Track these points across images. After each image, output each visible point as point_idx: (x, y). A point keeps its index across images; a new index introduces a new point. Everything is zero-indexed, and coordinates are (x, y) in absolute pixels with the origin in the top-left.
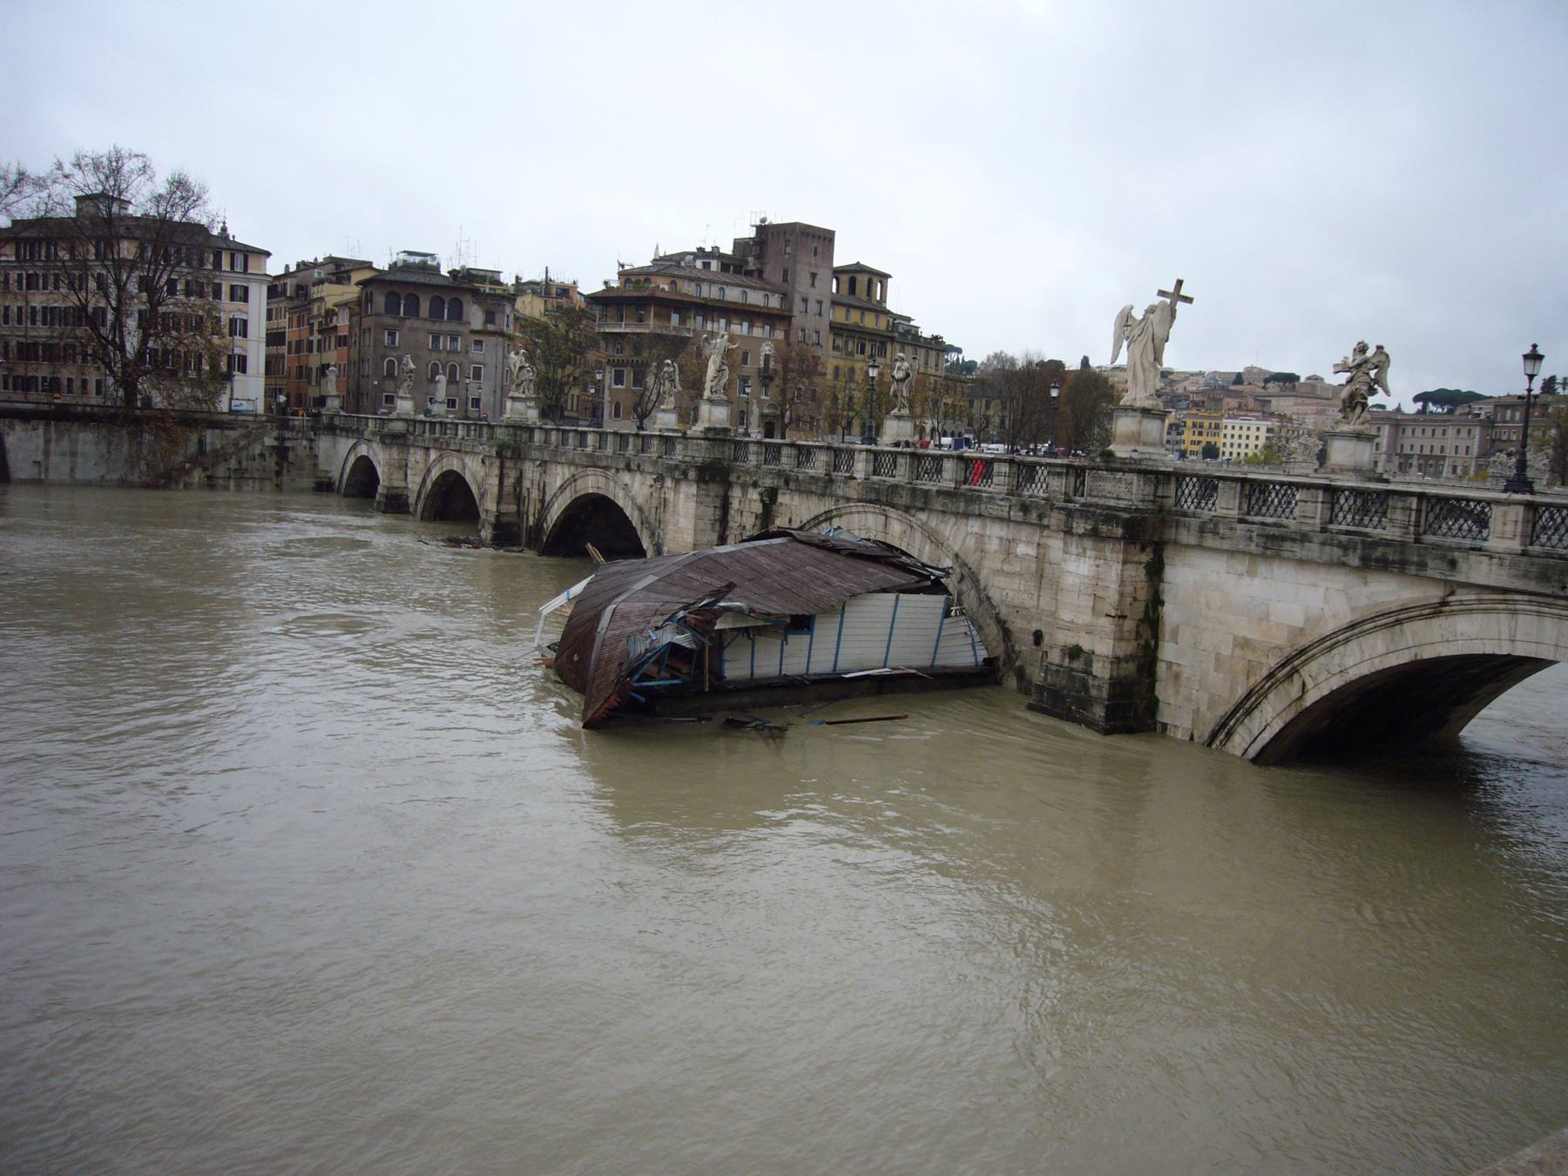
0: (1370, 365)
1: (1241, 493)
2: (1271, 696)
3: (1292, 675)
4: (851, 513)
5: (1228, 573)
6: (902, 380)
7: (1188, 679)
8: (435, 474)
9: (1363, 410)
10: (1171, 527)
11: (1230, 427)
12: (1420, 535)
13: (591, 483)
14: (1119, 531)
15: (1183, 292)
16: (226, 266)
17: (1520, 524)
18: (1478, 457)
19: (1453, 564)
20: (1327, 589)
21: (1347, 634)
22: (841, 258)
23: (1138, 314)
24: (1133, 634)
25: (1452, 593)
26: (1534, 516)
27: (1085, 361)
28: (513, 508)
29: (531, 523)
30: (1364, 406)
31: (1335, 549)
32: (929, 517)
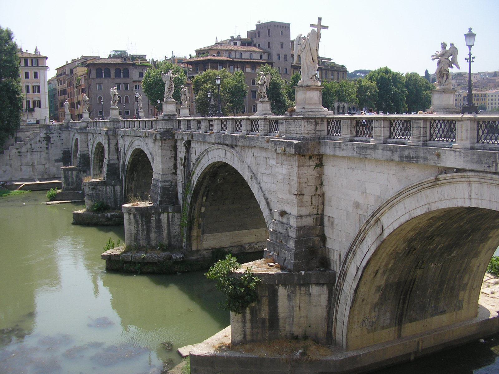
1: (350, 126)
2: (370, 233)
3: (377, 221)
5: (348, 168)
6: (261, 85)
10: (323, 146)
12: (427, 141)
14: (293, 151)
15: (322, 24)
16: (29, 64)
17: (469, 131)
19: (439, 156)
20: (388, 174)
24: (309, 203)
26: (478, 126)
27: (427, 72)
29: (122, 163)
30: (447, 76)
31: (388, 152)
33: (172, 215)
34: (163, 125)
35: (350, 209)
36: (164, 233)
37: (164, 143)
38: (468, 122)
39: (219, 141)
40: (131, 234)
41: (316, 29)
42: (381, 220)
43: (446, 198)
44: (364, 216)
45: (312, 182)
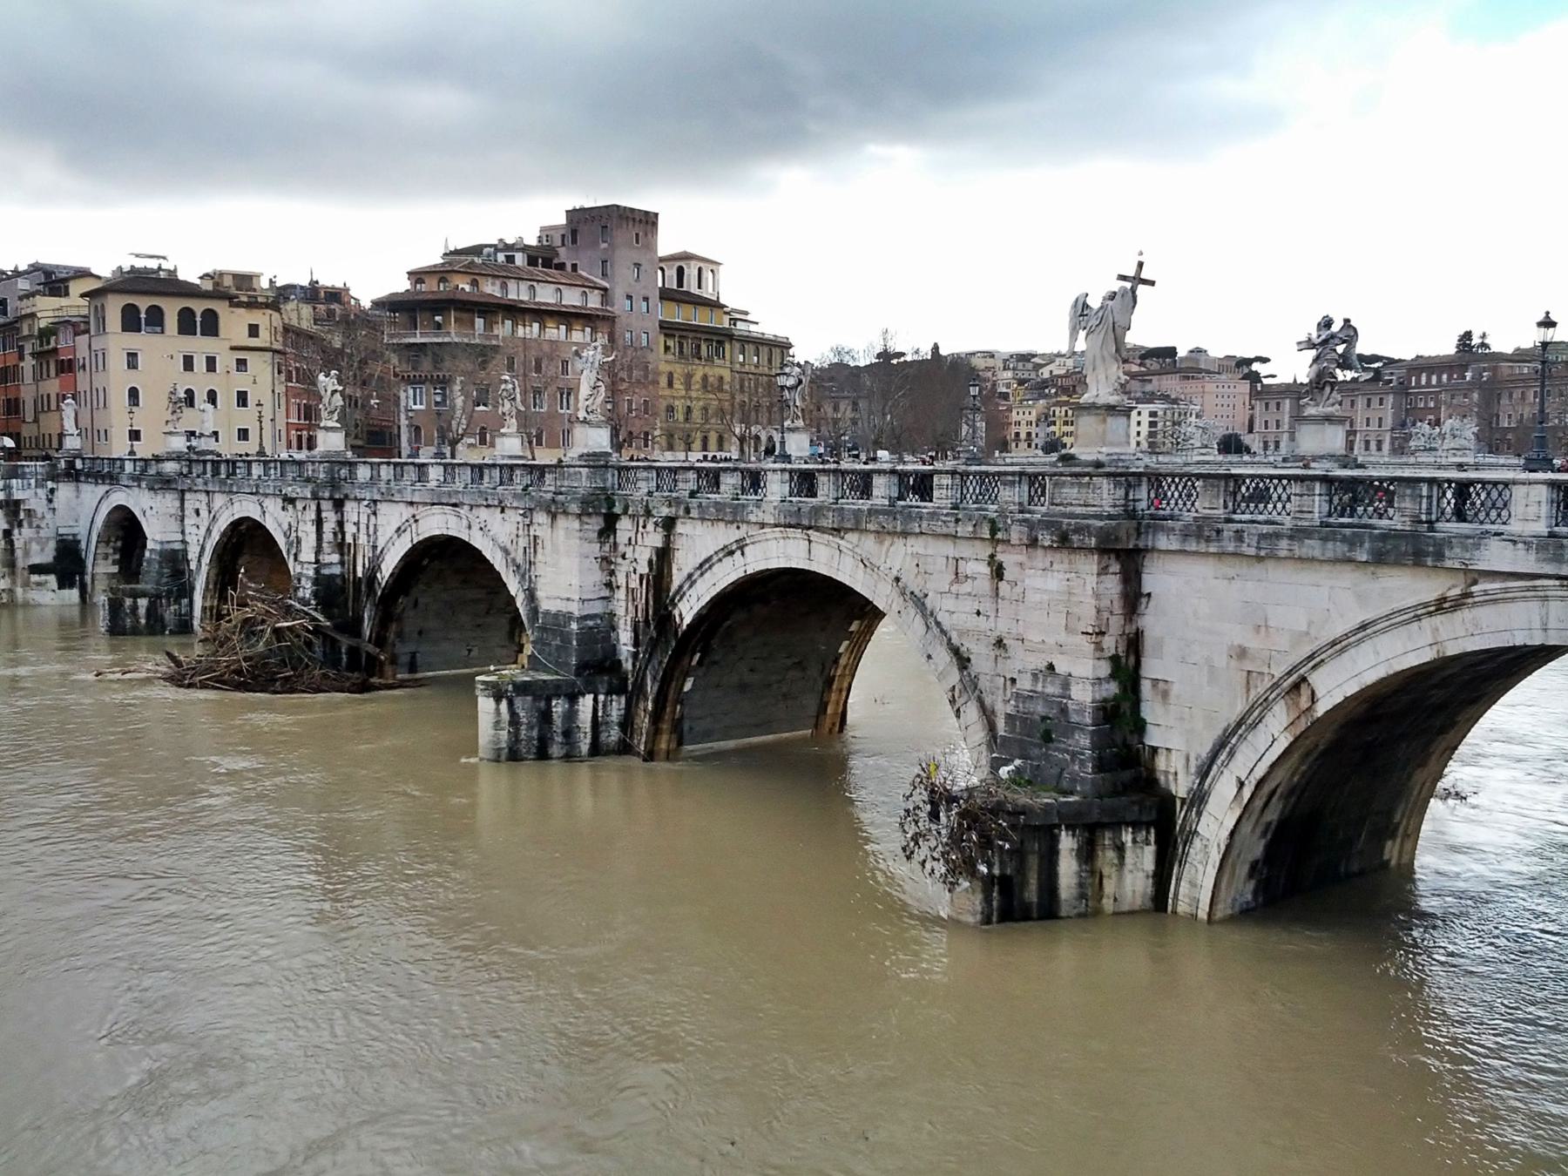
0: (1337, 341)
1: (1225, 491)
6: (794, 388)
7: (1178, 697)
8: (223, 524)
9: (1332, 390)
13: (436, 523)
18: (1393, 429)
20: (1331, 588)
21: (1360, 636)
22: (667, 243)
23: (1095, 302)
25: (1475, 582)
27: (936, 348)
28: (335, 558)
29: (360, 574)
32: (859, 540)
34: (584, 479)
35: (1221, 661)
36: (581, 744)
37: (587, 524)
38: (1544, 488)
39: (782, 521)
40: (499, 749)
41: (1128, 285)
42: (1310, 681)
43: (1485, 630)
44: (1261, 674)
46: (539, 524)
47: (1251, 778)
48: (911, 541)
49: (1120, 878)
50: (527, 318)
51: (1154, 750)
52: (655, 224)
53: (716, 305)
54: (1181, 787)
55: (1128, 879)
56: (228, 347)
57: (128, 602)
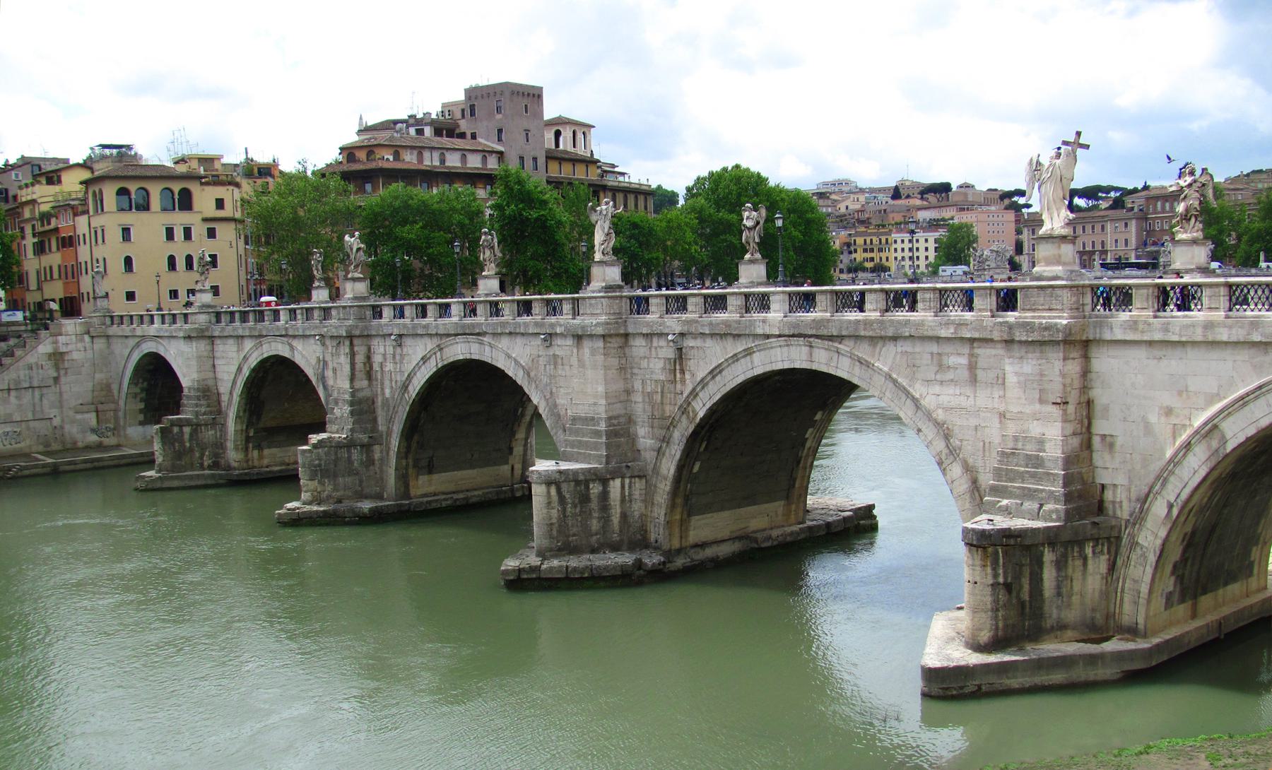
4: (772, 348)
5: (1148, 358)
7: (1122, 446)
8: (253, 361)
11: (899, 241)
18: (1136, 249)
22: (549, 113)
28: (365, 383)
33: (630, 482)
36: (613, 518)
37: (610, 342)
40: (552, 524)
41: (1070, 148)
45: (1077, 384)
46: (558, 346)
47: (1179, 501)
48: (900, 343)
49: (1084, 579)
50: (439, 180)
51: (1103, 486)
52: (540, 97)
53: (591, 162)
54: (1124, 513)
55: (1090, 580)
56: (200, 218)
57: (176, 429)
